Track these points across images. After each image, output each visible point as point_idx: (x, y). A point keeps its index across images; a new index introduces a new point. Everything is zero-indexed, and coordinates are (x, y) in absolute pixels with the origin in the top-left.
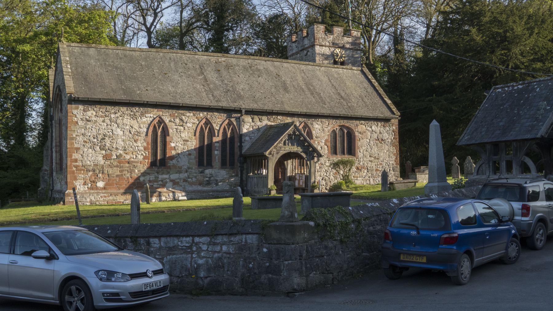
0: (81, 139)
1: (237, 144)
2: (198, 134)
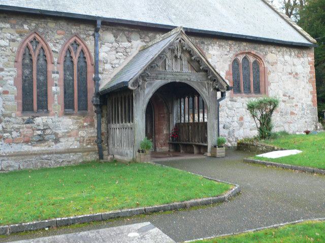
1: (91, 76)
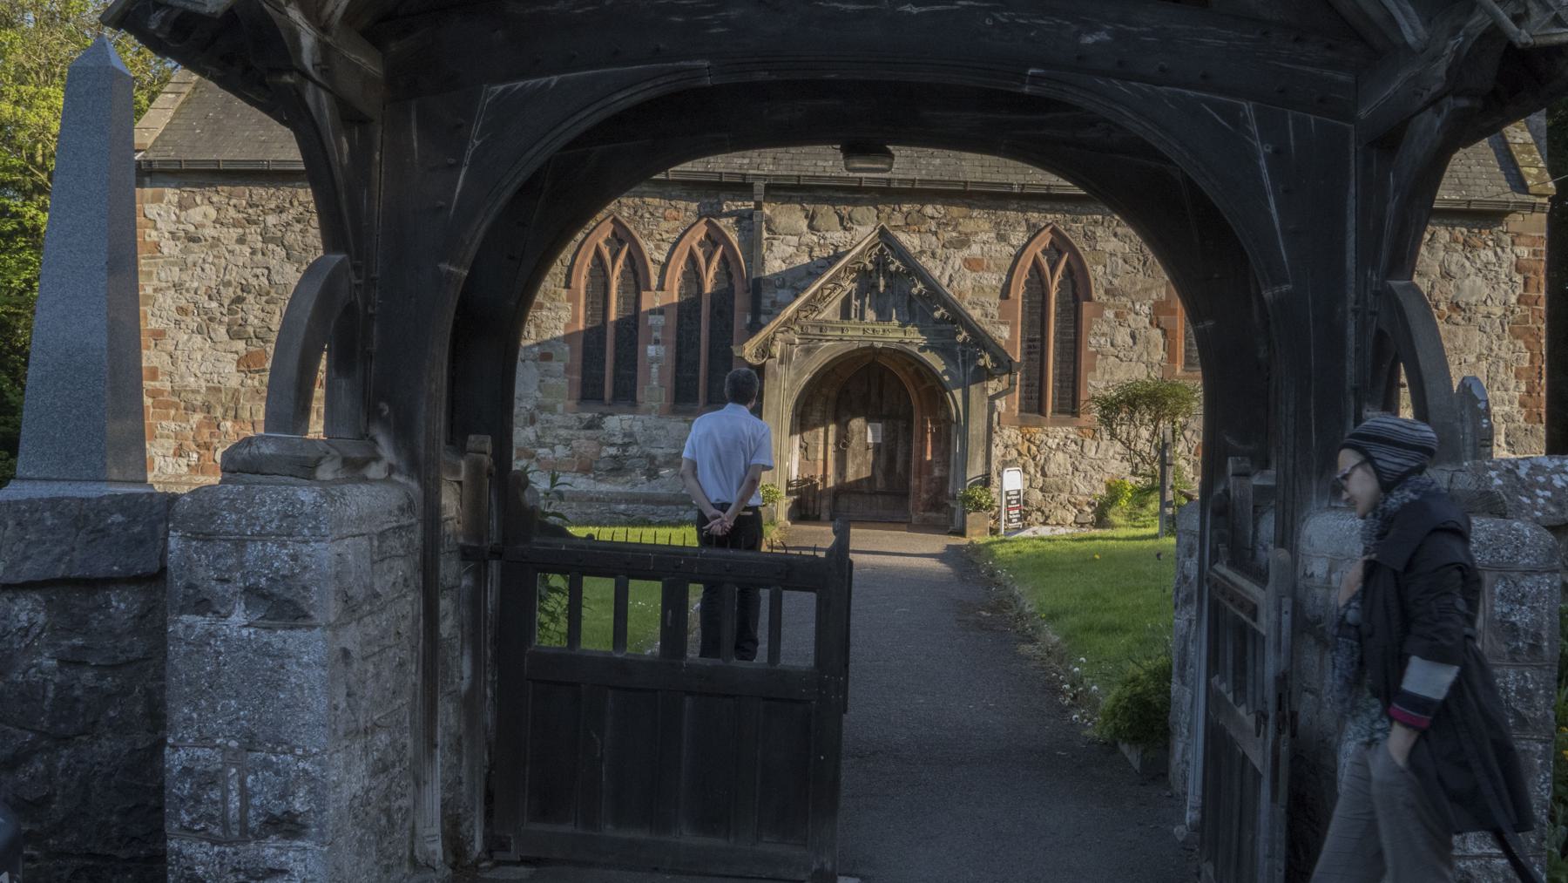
0: (168, 301)
2: (1018, 291)
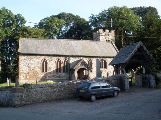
0: (22, 65)
